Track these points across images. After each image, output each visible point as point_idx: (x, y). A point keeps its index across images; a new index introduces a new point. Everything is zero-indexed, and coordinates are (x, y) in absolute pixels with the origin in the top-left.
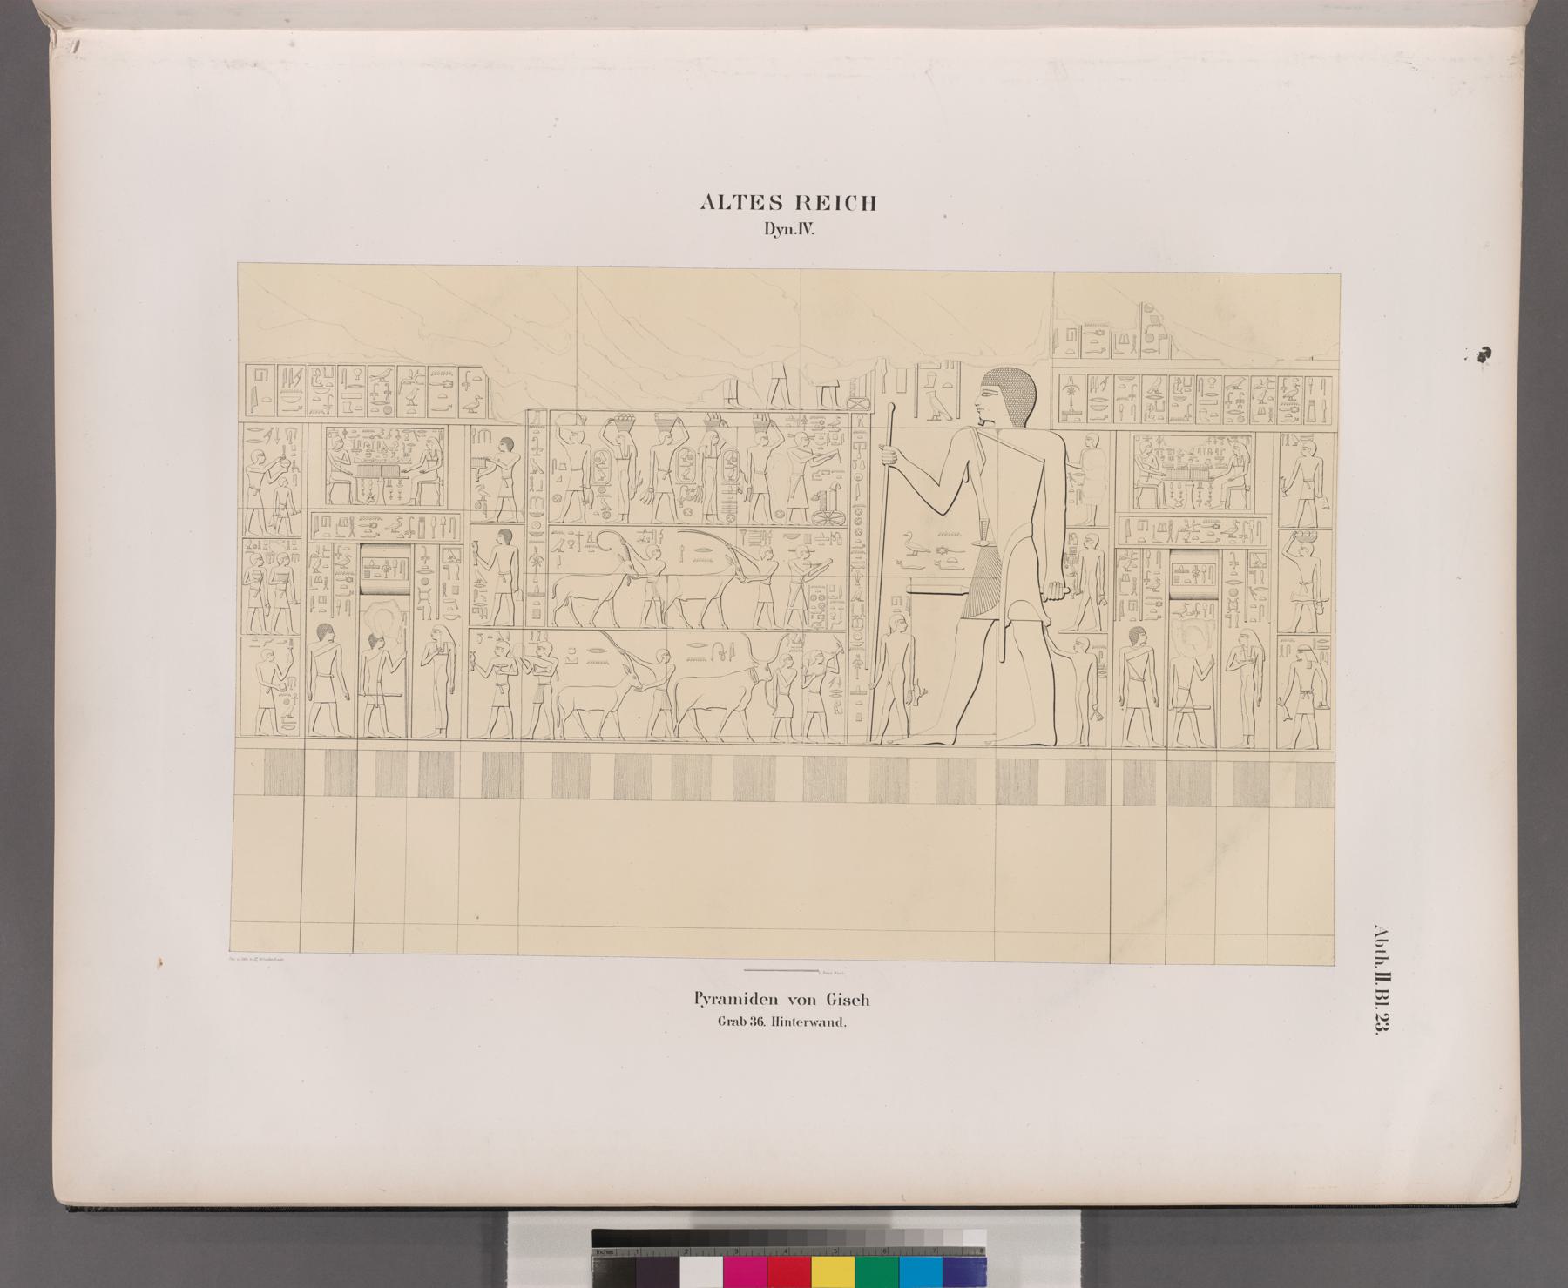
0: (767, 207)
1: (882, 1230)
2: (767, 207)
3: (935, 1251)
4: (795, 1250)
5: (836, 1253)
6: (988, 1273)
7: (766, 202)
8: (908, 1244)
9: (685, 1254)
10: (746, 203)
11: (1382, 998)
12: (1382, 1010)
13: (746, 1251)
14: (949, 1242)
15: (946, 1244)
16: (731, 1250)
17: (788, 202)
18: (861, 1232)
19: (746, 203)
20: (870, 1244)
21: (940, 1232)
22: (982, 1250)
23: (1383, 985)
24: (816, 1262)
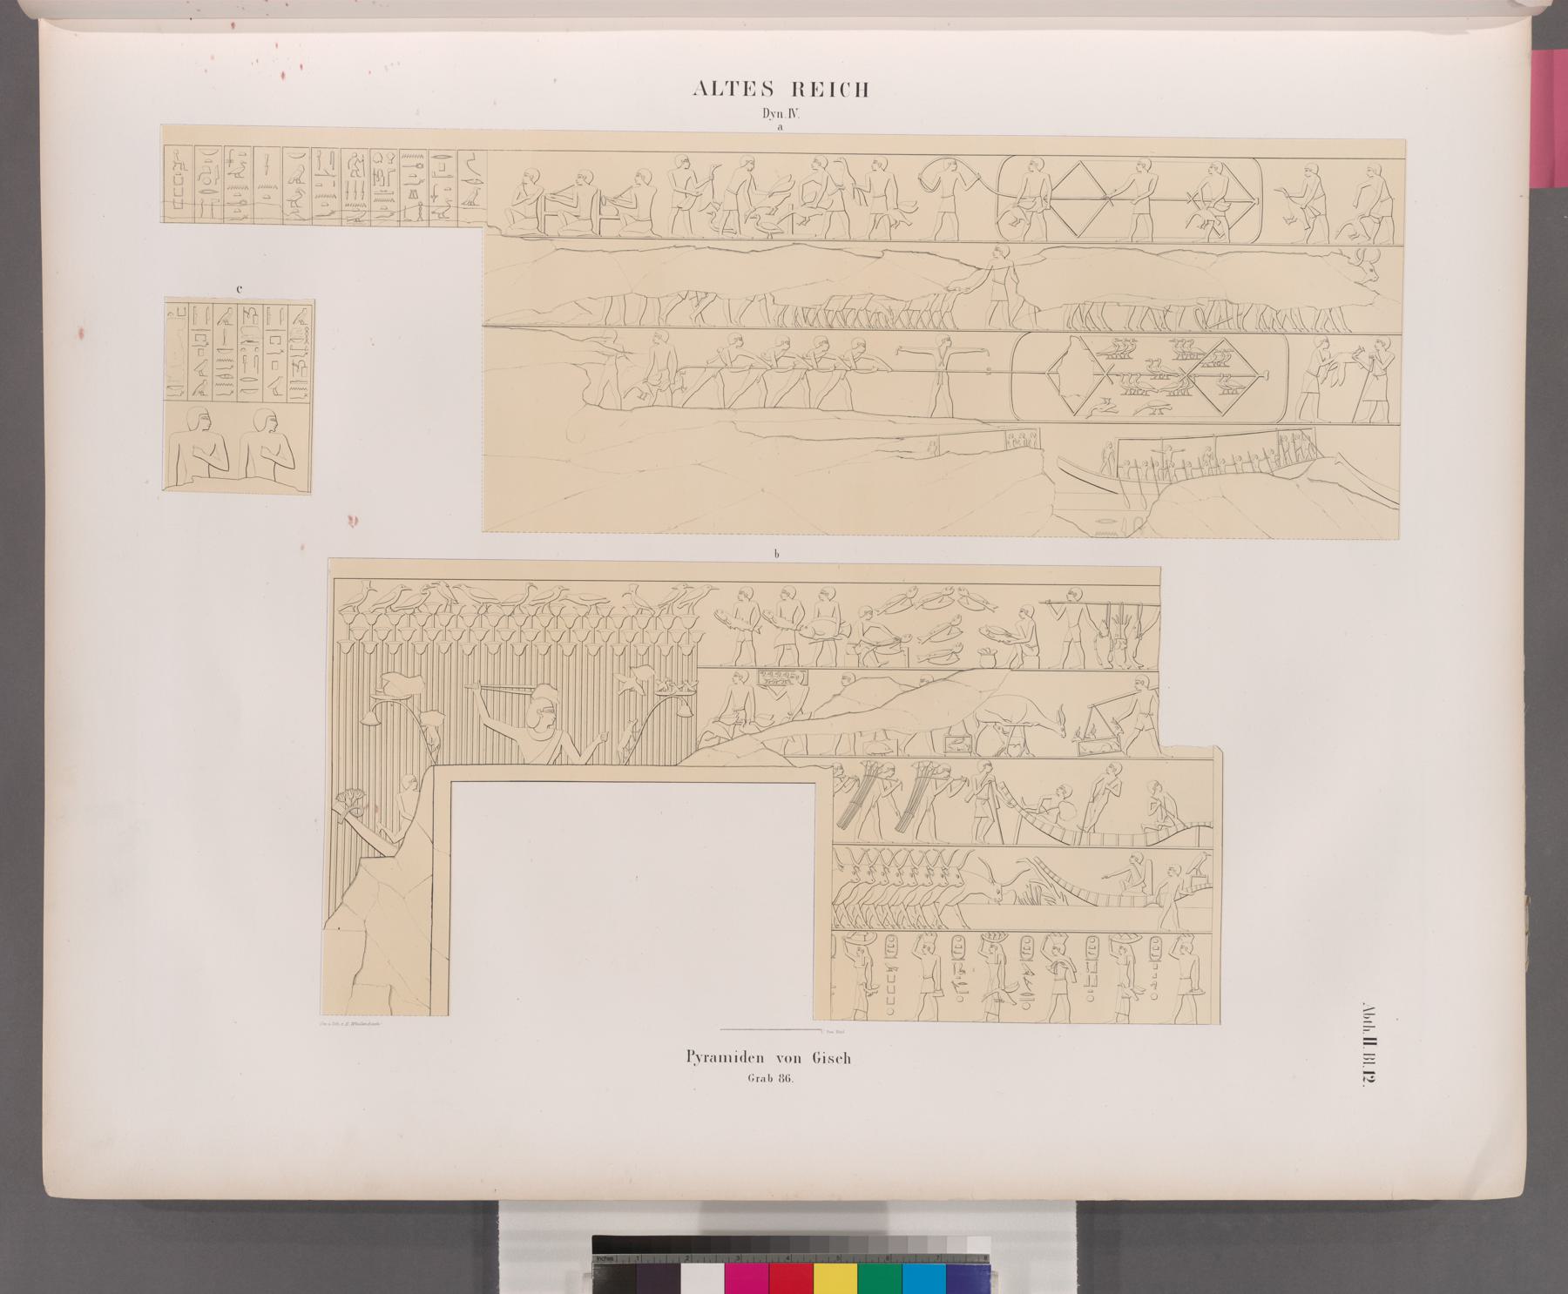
0: (759, 94)
1: (883, 1238)
2: (759, 94)
3: (938, 1256)
4: (797, 1257)
5: (839, 1260)
7: (759, 88)
8: (911, 1251)
10: (739, 90)
11: (1369, 1059)
12: (1369, 1068)
14: (952, 1249)
15: (949, 1252)
17: (783, 90)
18: (863, 1239)
19: (739, 90)
20: (873, 1251)
21: (943, 1239)
22: (986, 1257)
23: (1370, 1049)
24: (817, 1267)
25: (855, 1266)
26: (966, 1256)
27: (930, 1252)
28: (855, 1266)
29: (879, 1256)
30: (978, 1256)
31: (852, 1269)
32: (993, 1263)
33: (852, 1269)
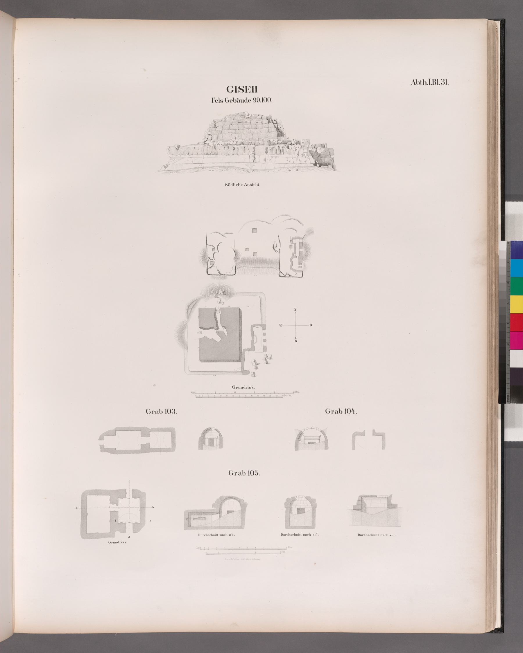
3: (508, 262)
4: (508, 320)
5: (509, 303)
6: (518, 240)
8: (505, 273)
9: (509, 365)
13: (508, 340)
15: (506, 258)
16: (507, 346)
20: (505, 289)
22: (508, 243)
24: (512, 311)
25: (511, 296)
26: (507, 251)
27: (506, 266)
28: (511, 296)
29: (507, 287)
30: (507, 246)
31: (512, 297)
32: (510, 240)
33: (512, 297)
